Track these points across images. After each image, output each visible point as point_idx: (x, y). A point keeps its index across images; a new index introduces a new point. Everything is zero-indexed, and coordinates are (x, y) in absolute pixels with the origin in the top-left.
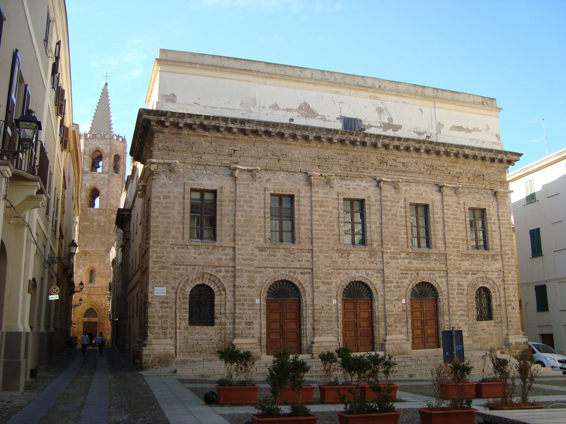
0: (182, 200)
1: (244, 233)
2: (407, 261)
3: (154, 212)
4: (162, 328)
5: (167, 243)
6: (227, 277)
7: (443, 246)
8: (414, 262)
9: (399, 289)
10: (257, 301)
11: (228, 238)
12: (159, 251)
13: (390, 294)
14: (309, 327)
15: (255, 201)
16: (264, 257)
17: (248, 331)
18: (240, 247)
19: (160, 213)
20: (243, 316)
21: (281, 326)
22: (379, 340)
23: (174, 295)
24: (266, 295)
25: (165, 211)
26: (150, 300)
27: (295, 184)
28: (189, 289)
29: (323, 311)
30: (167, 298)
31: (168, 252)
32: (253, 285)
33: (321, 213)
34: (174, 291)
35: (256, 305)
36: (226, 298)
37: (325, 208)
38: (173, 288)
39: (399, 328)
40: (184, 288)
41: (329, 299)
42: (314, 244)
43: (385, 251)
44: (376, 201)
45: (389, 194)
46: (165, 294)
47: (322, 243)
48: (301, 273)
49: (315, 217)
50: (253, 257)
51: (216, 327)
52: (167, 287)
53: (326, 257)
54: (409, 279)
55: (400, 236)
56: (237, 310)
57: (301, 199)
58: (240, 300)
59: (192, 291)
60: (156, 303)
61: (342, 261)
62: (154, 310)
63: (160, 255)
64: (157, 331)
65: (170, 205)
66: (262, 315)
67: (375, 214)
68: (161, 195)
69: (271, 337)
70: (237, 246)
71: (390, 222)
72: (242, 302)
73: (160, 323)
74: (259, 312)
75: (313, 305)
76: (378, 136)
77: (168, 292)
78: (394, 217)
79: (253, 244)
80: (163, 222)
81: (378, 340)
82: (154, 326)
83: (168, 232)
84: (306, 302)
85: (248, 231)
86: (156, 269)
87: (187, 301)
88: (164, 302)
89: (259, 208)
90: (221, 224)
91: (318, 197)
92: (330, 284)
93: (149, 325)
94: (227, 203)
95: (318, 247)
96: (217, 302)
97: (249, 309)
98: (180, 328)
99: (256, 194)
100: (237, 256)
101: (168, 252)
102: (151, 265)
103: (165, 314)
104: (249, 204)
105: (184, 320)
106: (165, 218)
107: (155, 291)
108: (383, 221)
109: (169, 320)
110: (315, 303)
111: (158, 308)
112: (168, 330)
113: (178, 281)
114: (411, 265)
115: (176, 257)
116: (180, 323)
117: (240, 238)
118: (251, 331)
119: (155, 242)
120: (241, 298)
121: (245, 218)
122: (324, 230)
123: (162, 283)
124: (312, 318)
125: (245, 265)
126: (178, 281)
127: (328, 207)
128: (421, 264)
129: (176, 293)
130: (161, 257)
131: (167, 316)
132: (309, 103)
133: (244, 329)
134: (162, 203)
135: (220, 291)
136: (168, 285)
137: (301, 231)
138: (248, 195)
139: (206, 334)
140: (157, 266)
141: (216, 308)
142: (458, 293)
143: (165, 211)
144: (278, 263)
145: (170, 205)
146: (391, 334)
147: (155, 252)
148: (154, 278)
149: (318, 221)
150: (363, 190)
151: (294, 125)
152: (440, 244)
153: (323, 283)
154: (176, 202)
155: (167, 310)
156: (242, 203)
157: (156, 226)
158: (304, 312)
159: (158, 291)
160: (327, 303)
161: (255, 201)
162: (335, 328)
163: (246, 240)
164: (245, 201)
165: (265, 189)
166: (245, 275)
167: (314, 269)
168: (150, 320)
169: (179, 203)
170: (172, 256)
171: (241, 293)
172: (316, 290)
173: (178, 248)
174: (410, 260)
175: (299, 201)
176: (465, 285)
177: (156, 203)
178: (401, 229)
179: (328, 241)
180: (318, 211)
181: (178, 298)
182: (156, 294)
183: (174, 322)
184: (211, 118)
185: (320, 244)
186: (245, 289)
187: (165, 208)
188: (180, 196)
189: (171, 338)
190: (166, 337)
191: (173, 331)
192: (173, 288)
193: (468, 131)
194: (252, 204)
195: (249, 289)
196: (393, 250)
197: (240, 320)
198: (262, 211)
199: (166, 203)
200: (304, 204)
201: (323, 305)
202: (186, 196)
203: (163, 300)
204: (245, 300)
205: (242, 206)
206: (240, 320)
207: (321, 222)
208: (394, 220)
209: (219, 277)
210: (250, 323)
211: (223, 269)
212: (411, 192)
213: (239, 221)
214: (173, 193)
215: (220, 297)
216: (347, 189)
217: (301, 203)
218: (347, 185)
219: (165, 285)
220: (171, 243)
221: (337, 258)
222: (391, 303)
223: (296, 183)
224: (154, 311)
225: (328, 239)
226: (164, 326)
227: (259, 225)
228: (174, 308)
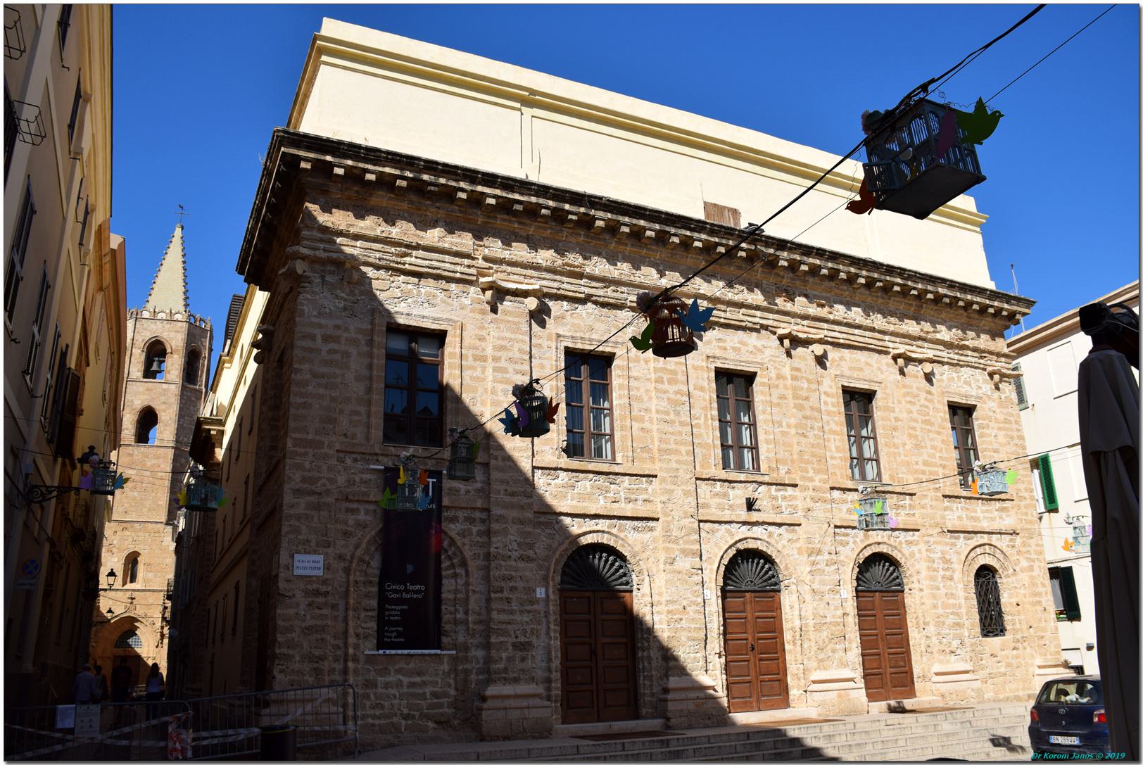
0: (365, 349)
3: (298, 371)
5: (330, 447)
6: (470, 534)
10: (540, 593)
12: (307, 465)
19: (315, 375)
20: (510, 627)
23: (341, 577)
24: (558, 578)
25: (326, 370)
26: (282, 585)
30: (325, 582)
32: (531, 553)
33: (672, 396)
34: (343, 565)
35: (537, 601)
36: (467, 584)
38: (341, 557)
46: (320, 573)
47: (677, 462)
52: (326, 555)
56: (494, 615)
58: (501, 591)
61: (719, 504)
62: (292, 611)
63: (310, 474)
64: (296, 666)
65: (338, 357)
66: (552, 626)
70: (493, 462)
71: (809, 423)
72: (506, 594)
77: (327, 567)
78: (816, 414)
82: (291, 652)
83: (333, 421)
86: (300, 510)
88: (317, 593)
93: (277, 651)
98: (355, 660)
100: (495, 486)
101: (330, 469)
102: (288, 498)
103: (319, 623)
107: (296, 564)
109: (328, 638)
111: (302, 606)
112: (326, 663)
113: (353, 541)
115: (351, 483)
116: (356, 647)
123: (313, 544)
125: (512, 506)
126: (353, 541)
129: (347, 571)
130: (312, 481)
131: (323, 629)
134: (318, 351)
135: (453, 566)
136: (330, 550)
140: (302, 502)
143: (326, 370)
145: (338, 357)
148: (297, 531)
153: (683, 551)
154: (353, 351)
155: (325, 611)
166: (513, 529)
168: (280, 638)
170: (341, 479)
171: (504, 572)
173: (355, 460)
176: (954, 560)
177: (303, 348)
182: (297, 572)
183: (340, 642)
185: (675, 465)
186: (513, 563)
191: (338, 666)
195: (521, 565)
196: (817, 483)
197: (502, 639)
199: (330, 352)
202: (376, 338)
203: (315, 586)
204: (513, 589)
206: (502, 639)
207: (672, 416)
210: (524, 647)
211: (461, 514)
212: (843, 363)
214: (347, 330)
215: (453, 581)
216: (720, 348)
218: (720, 339)
220: (338, 447)
222: (821, 599)
224: (293, 614)
228: (342, 608)
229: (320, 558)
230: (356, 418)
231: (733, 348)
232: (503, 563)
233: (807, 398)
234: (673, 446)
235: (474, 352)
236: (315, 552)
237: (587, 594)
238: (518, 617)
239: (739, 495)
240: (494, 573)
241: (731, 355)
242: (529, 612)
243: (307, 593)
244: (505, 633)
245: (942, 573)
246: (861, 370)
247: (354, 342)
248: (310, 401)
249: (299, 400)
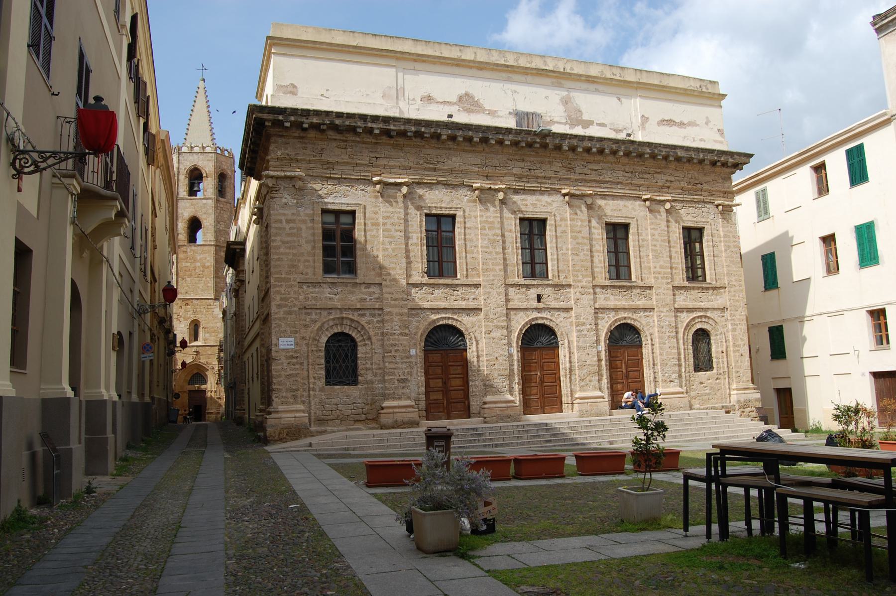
0: (310, 225)
4: (291, 390)
8: (612, 297)
10: (413, 352)
11: (373, 273)
19: (284, 242)
21: (444, 383)
23: (304, 348)
24: (423, 344)
25: (289, 239)
26: (274, 354)
28: (324, 339)
30: (296, 351)
31: (295, 292)
32: (407, 331)
33: (492, 237)
35: (411, 356)
51: (359, 386)
52: (296, 338)
58: (390, 352)
59: (328, 341)
61: (519, 299)
62: (280, 367)
64: (284, 394)
65: (295, 231)
68: (283, 218)
70: (384, 283)
71: (581, 247)
72: (393, 353)
73: (288, 383)
76: (564, 136)
77: (297, 344)
86: (281, 315)
87: (323, 354)
88: (292, 357)
98: (314, 390)
100: (386, 295)
101: (295, 292)
102: (274, 309)
105: (319, 378)
106: (289, 248)
115: (307, 299)
116: (314, 383)
119: (277, 280)
125: (396, 306)
126: (310, 329)
130: (286, 299)
131: (296, 375)
133: (396, 388)
134: (284, 229)
135: (364, 340)
139: (348, 396)
143: (289, 239)
145: (295, 231)
147: (279, 293)
148: (280, 326)
151: (453, 123)
154: (303, 226)
155: (297, 366)
157: (278, 260)
159: (285, 343)
166: (396, 319)
168: (274, 381)
169: (307, 228)
173: (308, 287)
177: (276, 228)
182: (281, 347)
183: (306, 382)
185: (492, 278)
187: (289, 235)
189: (303, 402)
190: (296, 402)
191: (306, 394)
195: (401, 337)
196: (584, 284)
199: (290, 229)
207: (491, 249)
209: (363, 323)
211: (367, 312)
214: (299, 215)
224: (280, 369)
228: (305, 364)
233: (580, 232)
234: (492, 267)
236: (290, 337)
239: (533, 293)
241: (530, 209)
243: (287, 358)
244: (393, 374)
247: (304, 222)
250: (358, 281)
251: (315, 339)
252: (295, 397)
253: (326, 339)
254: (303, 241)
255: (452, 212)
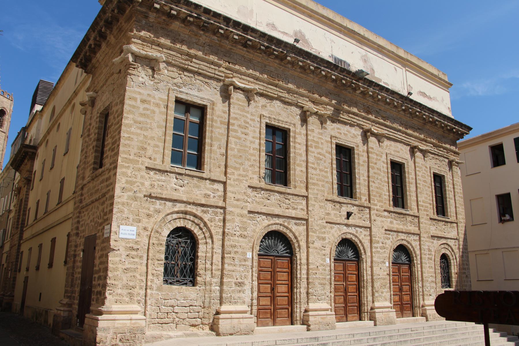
1: (238, 166)
2: (389, 220)
3: (127, 118)
4: (126, 287)
5: (142, 164)
6: (215, 220)
7: (416, 207)
8: (395, 222)
9: (384, 250)
11: (218, 170)
12: (130, 175)
13: (377, 255)
14: (303, 291)
15: (250, 128)
16: (257, 200)
17: (238, 295)
18: (232, 183)
19: (136, 122)
20: (234, 273)
21: (273, 289)
22: (366, 308)
26: (112, 243)
27: (290, 117)
28: (166, 232)
29: (317, 272)
30: (137, 243)
31: (142, 177)
32: (245, 233)
33: (316, 155)
36: (213, 248)
37: (320, 150)
39: (385, 293)
40: (160, 230)
41: (323, 257)
42: (309, 191)
43: (372, 206)
44: (363, 151)
45: (374, 147)
46: (134, 237)
47: (317, 190)
48: (296, 224)
49: (311, 159)
50: (246, 198)
51: (197, 287)
53: (321, 207)
54: (391, 239)
55: (383, 193)
57: (297, 136)
58: (230, 253)
59: (169, 236)
60: (122, 249)
62: (117, 259)
63: (130, 179)
64: (119, 291)
65: (148, 112)
67: (363, 165)
68: (139, 97)
69: (261, 303)
70: (228, 181)
71: (376, 176)
72: (232, 255)
73: (125, 279)
74: (251, 270)
75: (308, 264)
77: (138, 235)
78: (379, 172)
79: (247, 181)
80: (138, 135)
81: (366, 308)
82: (116, 283)
84: (300, 259)
85: (242, 164)
86: (124, 199)
87: (163, 249)
88: (132, 249)
89: (253, 138)
90: (211, 150)
91: (314, 137)
92: (324, 239)
94: (218, 124)
95: (313, 194)
96: (201, 253)
97: (240, 265)
99: (251, 120)
100: (229, 194)
102: (118, 192)
103: (133, 266)
104: (243, 130)
106: (141, 129)
107: (121, 231)
108: (370, 175)
110: (310, 261)
111: (124, 256)
112: (136, 290)
114: (392, 226)
115: (152, 186)
117: (233, 171)
118: (241, 295)
119: (126, 160)
120: (231, 249)
121: (238, 147)
122: (319, 175)
123: (131, 220)
124: (306, 280)
125: (237, 206)
126: (152, 220)
127: (322, 149)
128: (400, 225)
130: (132, 183)
131: (135, 270)
132: (303, 31)
133: (233, 291)
136: (140, 224)
137: (297, 173)
138: (243, 119)
139: (185, 298)
141: (199, 261)
142: (428, 258)
144: (273, 209)
145: (148, 112)
146: (378, 301)
147: (124, 174)
148: (122, 211)
149: (313, 164)
150: (352, 137)
152: (414, 205)
153: (318, 237)
154: (156, 109)
155: (136, 260)
156: (236, 127)
157: (129, 138)
158: (299, 272)
160: (322, 262)
161: (250, 128)
162: (328, 294)
163: (240, 175)
164: (239, 126)
165: (261, 116)
166: (237, 219)
167: (310, 220)
169: (161, 112)
170: (147, 183)
171: (232, 243)
172: (311, 245)
174: (392, 220)
175: (295, 138)
176: (433, 250)
177: (130, 105)
178: (383, 186)
179: (323, 189)
180: (313, 152)
181: (151, 244)
182: (121, 236)
184: (212, 14)
185: (316, 191)
186: (237, 238)
187: (142, 115)
188: (162, 104)
192: (145, 229)
193: (430, 98)
194: (246, 131)
195: (241, 239)
196: (378, 207)
197: (229, 280)
198: (257, 141)
199: (145, 109)
200: (299, 141)
201: (318, 265)
202: (169, 104)
203: (131, 245)
204: (236, 252)
205: (236, 131)
206: (229, 280)
208: (379, 174)
209: (206, 220)
210: (240, 284)
213: (233, 149)
215: (205, 246)
216: (338, 133)
217: (296, 140)
218: (338, 129)
219: (135, 224)
220: (147, 165)
221: (330, 209)
222: (378, 266)
223: (292, 116)
225: (323, 186)
226: (131, 284)
227: (253, 158)
228: (145, 258)
229: (134, 228)
230: (156, 149)
231: (344, 134)
232: (232, 238)
233: (376, 164)
234: (316, 182)
235: (221, 119)
236: (132, 225)
237: (271, 257)
238: (238, 268)
239: (345, 209)
240: (227, 243)
241: (342, 137)
242: (244, 265)
244: (231, 277)
245: (428, 256)
246: (399, 152)
247: (158, 105)
248: (132, 136)
249: (126, 135)
250: (204, 175)
251: (157, 232)
252: (131, 295)
253: (168, 232)
254: (155, 125)
255: (287, 126)
